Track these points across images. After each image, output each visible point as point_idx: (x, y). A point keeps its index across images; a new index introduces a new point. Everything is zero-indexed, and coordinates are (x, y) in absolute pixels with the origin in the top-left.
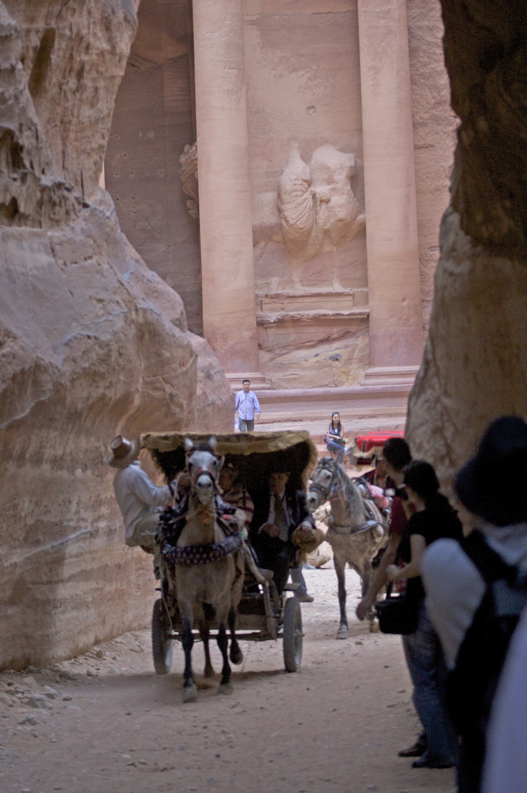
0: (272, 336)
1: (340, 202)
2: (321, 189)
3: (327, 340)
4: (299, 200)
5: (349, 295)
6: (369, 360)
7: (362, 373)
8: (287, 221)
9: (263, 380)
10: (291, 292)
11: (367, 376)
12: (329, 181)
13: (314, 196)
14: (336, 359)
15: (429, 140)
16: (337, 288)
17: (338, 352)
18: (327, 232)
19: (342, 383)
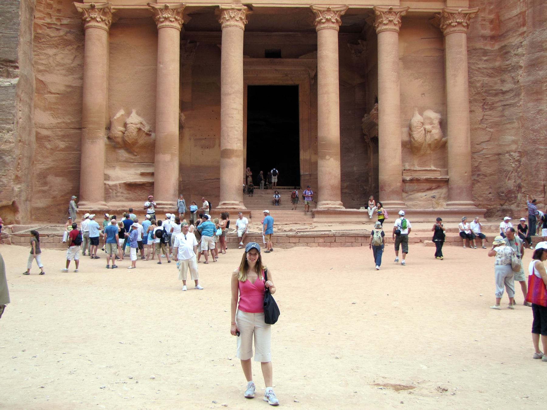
0: (408, 186)
1: (436, 132)
2: (428, 127)
3: (430, 189)
4: (419, 130)
5: (439, 171)
6: (449, 197)
7: (445, 203)
8: (414, 139)
9: (404, 204)
10: (415, 169)
11: (447, 205)
12: (431, 123)
13: (425, 129)
14: (434, 197)
15: (473, 108)
16: (433, 168)
17: (434, 194)
18: (429, 145)
19: (436, 208)
